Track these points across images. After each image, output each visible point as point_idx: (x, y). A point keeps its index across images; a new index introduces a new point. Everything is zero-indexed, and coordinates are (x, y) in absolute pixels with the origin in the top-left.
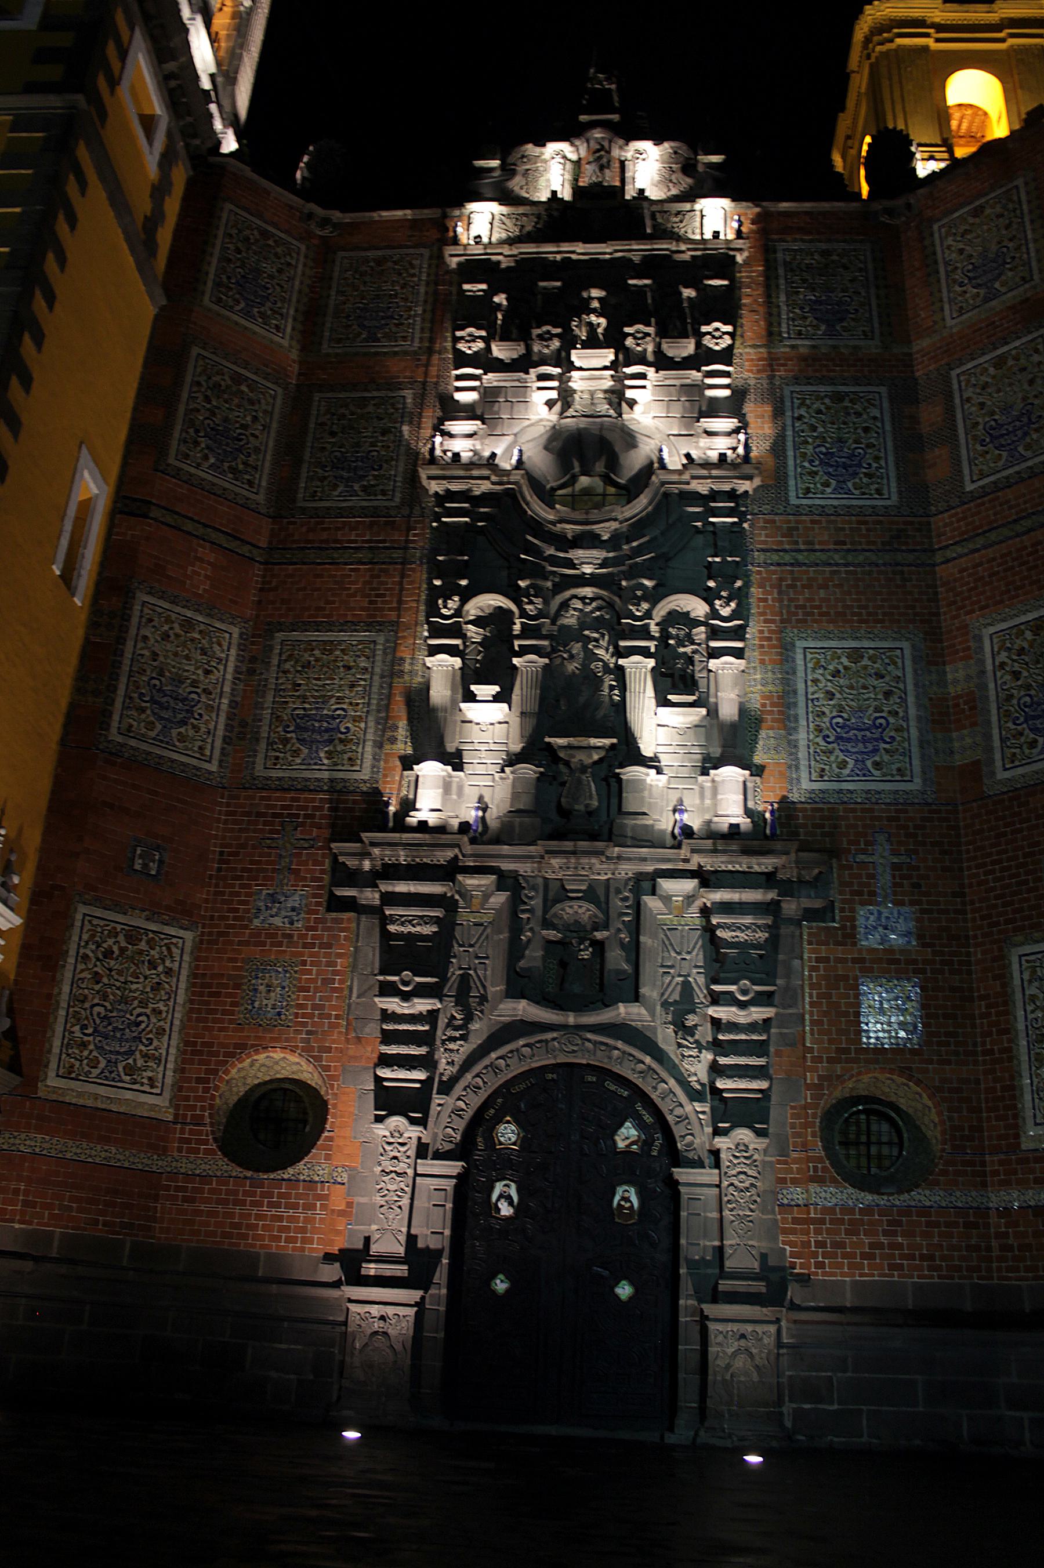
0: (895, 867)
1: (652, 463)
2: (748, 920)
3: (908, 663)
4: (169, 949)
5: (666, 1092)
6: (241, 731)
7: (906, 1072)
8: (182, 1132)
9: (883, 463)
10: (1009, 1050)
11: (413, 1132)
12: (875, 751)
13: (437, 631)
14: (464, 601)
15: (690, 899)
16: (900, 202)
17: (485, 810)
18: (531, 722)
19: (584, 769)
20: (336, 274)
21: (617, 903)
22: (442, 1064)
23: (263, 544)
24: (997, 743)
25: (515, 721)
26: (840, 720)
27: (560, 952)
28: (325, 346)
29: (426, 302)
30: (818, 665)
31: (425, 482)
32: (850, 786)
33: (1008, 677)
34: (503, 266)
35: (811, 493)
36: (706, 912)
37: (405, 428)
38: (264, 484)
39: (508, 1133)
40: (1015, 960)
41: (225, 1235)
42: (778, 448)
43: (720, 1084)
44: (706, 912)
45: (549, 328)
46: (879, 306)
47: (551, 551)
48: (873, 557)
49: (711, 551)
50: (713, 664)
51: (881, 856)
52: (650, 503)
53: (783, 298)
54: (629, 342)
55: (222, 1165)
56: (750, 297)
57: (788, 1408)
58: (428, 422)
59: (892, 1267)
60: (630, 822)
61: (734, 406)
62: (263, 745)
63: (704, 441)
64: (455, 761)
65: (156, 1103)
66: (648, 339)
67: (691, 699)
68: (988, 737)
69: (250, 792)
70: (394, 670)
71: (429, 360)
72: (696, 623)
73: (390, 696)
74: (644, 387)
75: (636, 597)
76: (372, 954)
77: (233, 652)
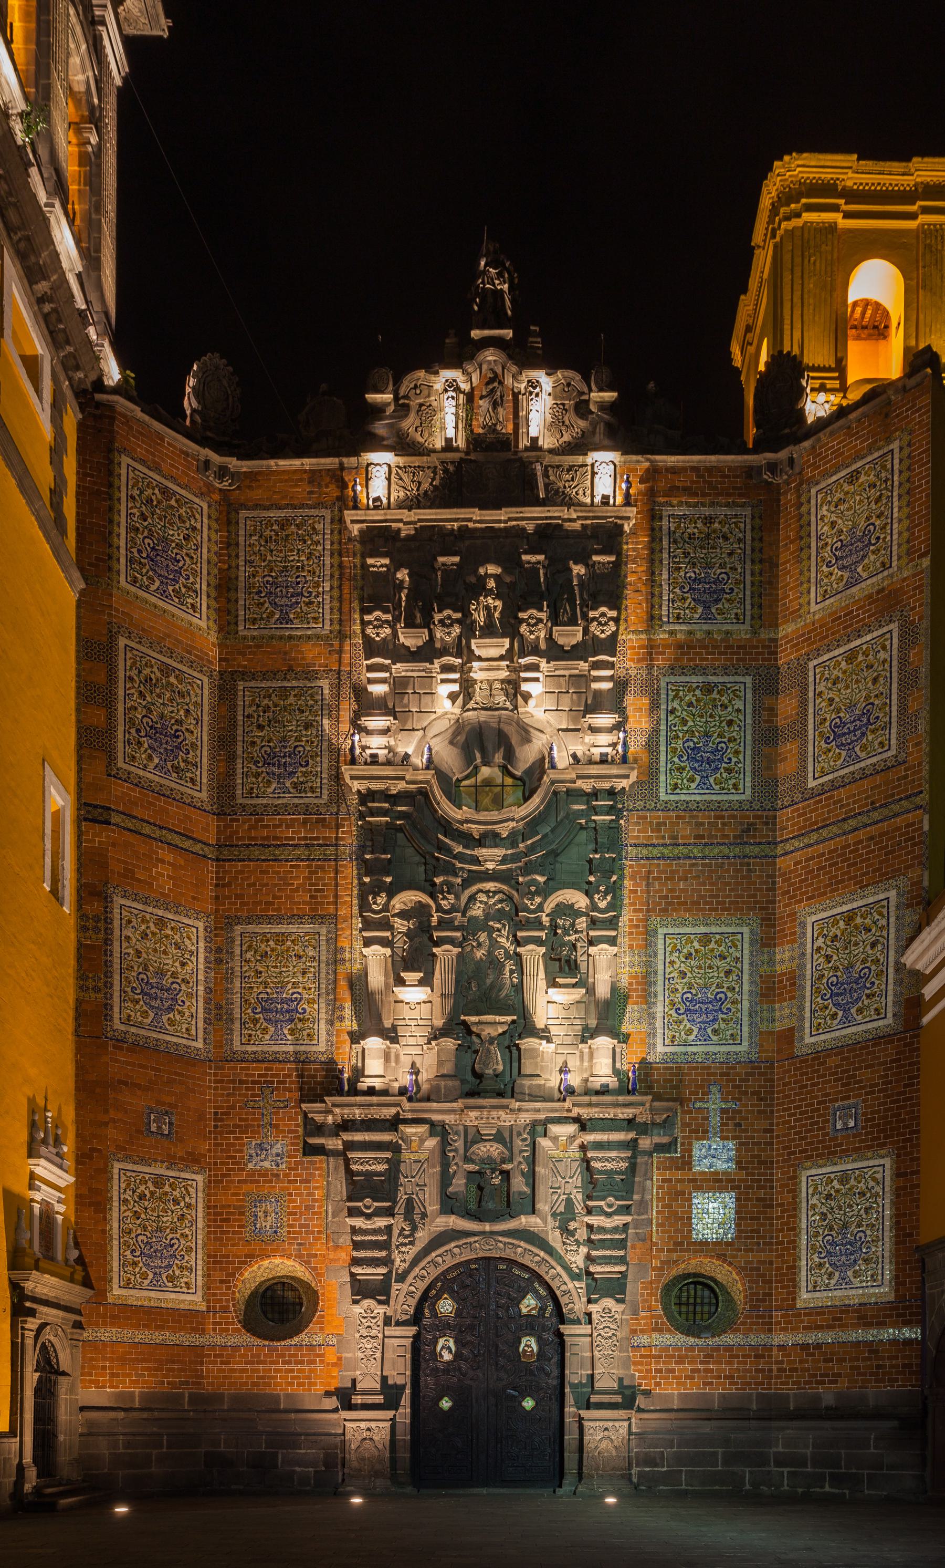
0: (723, 1111)
1: (543, 758)
2: (613, 1154)
3: (746, 946)
4: (186, 1189)
5: (555, 1274)
6: (218, 1013)
7: (722, 1257)
8: (214, 1317)
9: (741, 757)
10: (795, 1241)
11: (380, 1310)
12: (715, 1020)
13: (368, 925)
14: (390, 897)
15: (572, 1138)
16: (783, 455)
17: (417, 1073)
18: (450, 1003)
19: (491, 1040)
20: (241, 539)
21: (518, 1143)
22: (397, 1262)
23: (213, 842)
24: (808, 1015)
25: (437, 1001)
26: (689, 995)
27: (477, 1179)
28: (241, 628)
29: (332, 576)
30: (675, 949)
31: (348, 780)
32: (694, 1049)
33: (822, 960)
34: (403, 534)
35: (677, 789)
36: (583, 1148)
37: (326, 722)
38: (205, 780)
40: (804, 1179)
41: (254, 1384)
42: (651, 746)
43: (592, 1269)
44: (583, 1148)
45: (450, 612)
46: (753, 584)
47: (459, 849)
48: (726, 850)
49: (592, 846)
50: (592, 950)
51: (714, 1104)
52: (542, 803)
53: (665, 576)
54: (523, 629)
55: (246, 1338)
56: (635, 573)
57: (635, 1470)
58: (346, 716)
59: (705, 1384)
60: (527, 1082)
61: (614, 701)
62: (237, 1025)
63: (589, 738)
64: (391, 1035)
65: (194, 1300)
66: (541, 625)
67: (574, 981)
68: (801, 1008)
69: (232, 1064)
70: (336, 960)
71: (341, 646)
72: (578, 913)
73: (335, 981)
74: (537, 680)
75: (530, 892)
76: (340, 1186)
77: (201, 944)
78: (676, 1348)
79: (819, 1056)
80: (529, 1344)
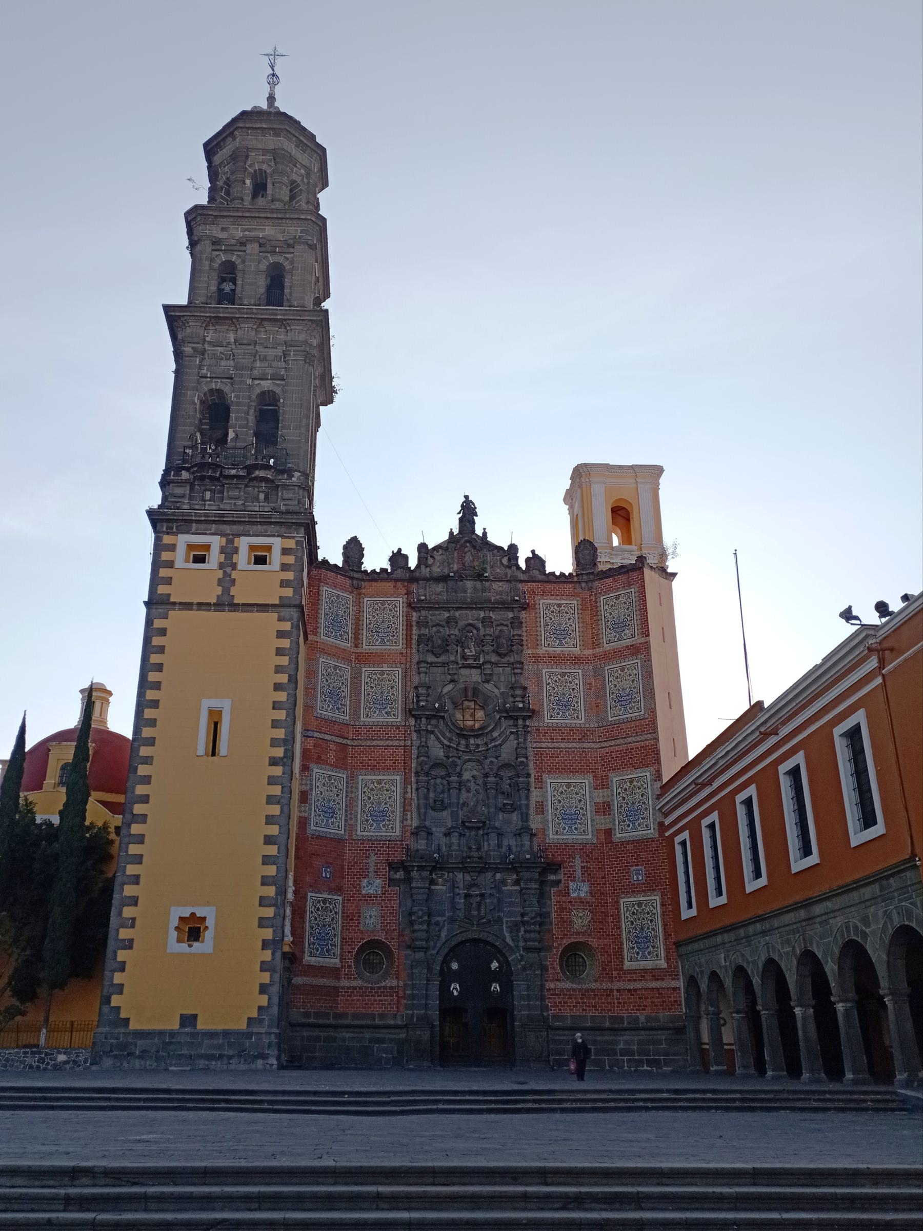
0: (582, 867)
39: (455, 966)
59: (583, 1010)
78: (568, 990)
79: (624, 843)
80: (496, 987)
